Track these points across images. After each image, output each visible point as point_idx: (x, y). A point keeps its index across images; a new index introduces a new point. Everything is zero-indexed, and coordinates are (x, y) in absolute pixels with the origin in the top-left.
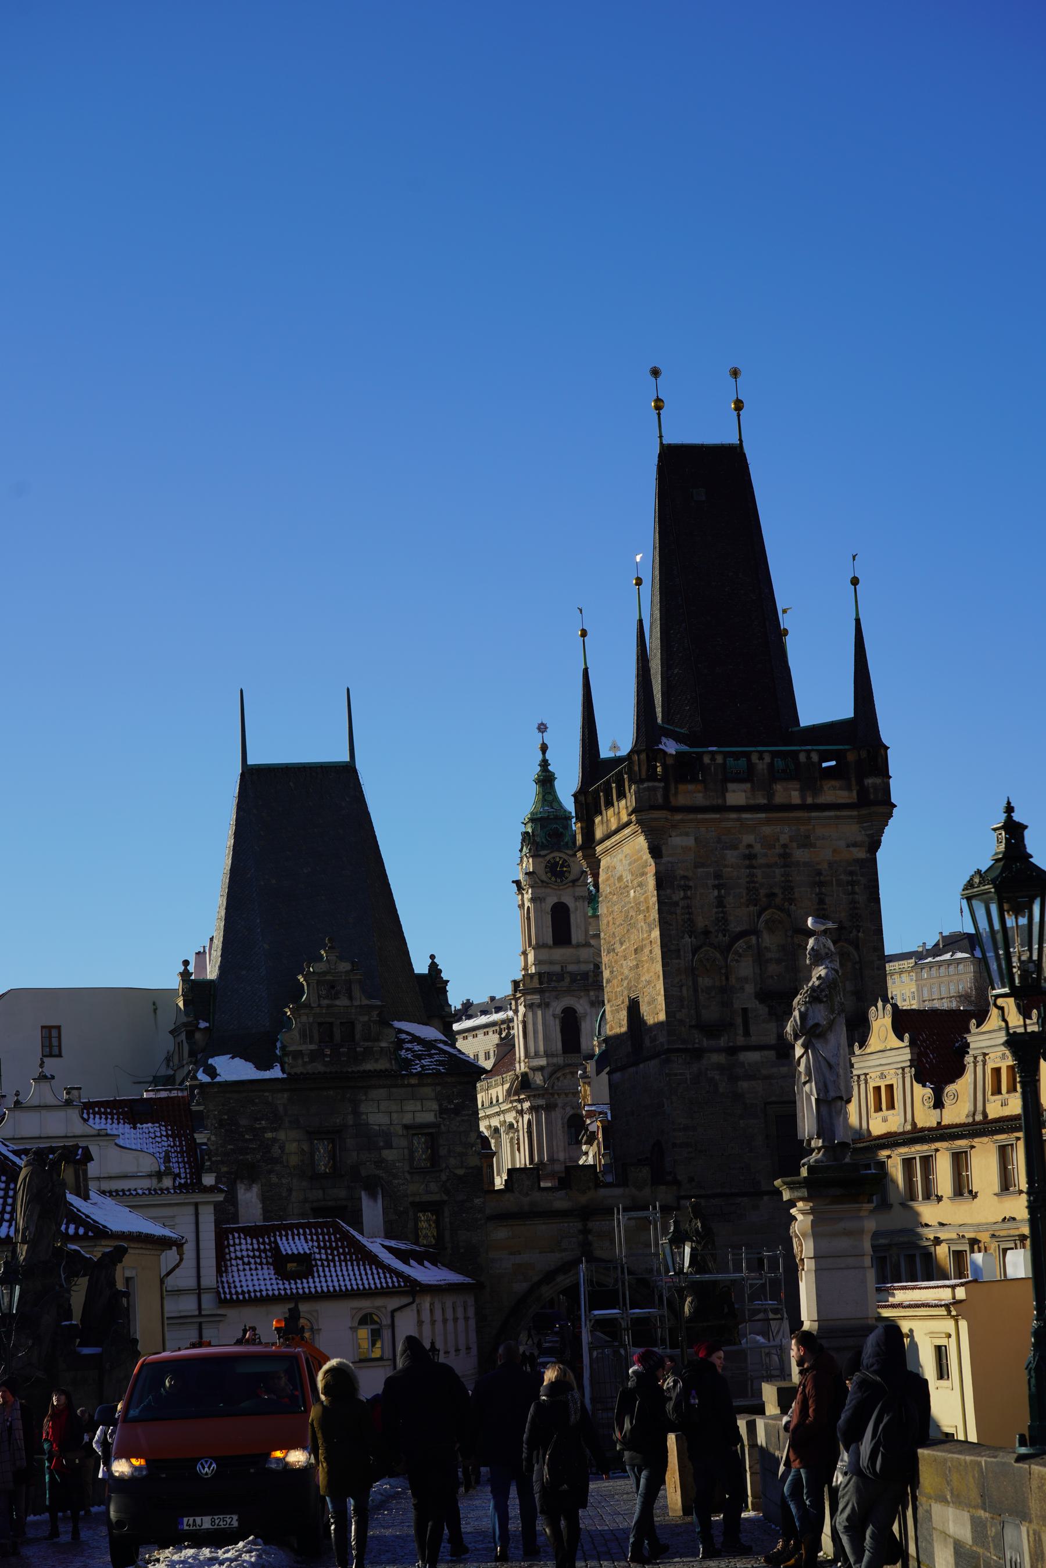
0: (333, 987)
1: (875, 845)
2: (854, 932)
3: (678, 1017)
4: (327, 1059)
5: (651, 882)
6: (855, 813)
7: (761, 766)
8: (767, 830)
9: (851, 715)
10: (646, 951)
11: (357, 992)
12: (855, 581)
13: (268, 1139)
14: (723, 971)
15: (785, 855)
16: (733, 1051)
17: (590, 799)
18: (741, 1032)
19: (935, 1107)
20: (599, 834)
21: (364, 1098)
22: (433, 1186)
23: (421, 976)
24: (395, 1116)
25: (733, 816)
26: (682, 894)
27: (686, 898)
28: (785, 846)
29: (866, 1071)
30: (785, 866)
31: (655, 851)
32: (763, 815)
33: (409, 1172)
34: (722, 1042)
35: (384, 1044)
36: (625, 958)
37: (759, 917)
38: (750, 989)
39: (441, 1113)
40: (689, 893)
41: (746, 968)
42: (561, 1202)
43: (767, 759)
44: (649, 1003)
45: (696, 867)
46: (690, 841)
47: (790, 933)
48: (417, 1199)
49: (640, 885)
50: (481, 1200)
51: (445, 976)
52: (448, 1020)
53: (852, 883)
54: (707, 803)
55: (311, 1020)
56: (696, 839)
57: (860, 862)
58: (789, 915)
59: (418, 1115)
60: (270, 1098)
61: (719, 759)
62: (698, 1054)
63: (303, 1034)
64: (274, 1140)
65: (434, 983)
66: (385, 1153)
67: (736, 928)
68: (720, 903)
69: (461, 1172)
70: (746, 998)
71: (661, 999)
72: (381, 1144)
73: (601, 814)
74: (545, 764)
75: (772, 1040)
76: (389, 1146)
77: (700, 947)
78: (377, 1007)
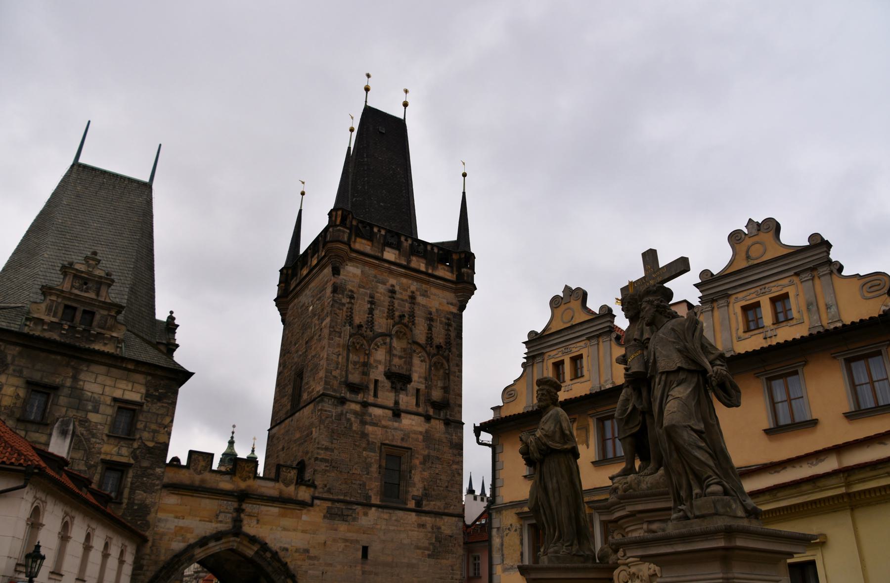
1: (462, 307)
2: (447, 352)
3: (334, 373)
5: (329, 290)
7: (406, 244)
8: (404, 280)
9: (455, 238)
11: (103, 292)
12: (464, 175)
15: (413, 298)
16: (365, 405)
17: (290, 272)
18: (372, 393)
21: (85, 369)
22: (125, 451)
24: (107, 389)
25: (386, 265)
28: (413, 292)
29: (544, 351)
33: (108, 436)
34: (360, 397)
35: (114, 334)
36: (297, 352)
37: (393, 326)
38: (381, 368)
39: (146, 397)
41: (380, 355)
42: (226, 484)
43: (410, 242)
44: (312, 370)
47: (410, 341)
48: (108, 458)
49: (319, 299)
50: (162, 470)
51: (176, 322)
54: (372, 253)
56: (362, 271)
57: (454, 315)
61: (383, 232)
62: (343, 401)
63: (49, 310)
68: (371, 312)
69: (151, 444)
70: (378, 373)
71: (323, 363)
72: (90, 408)
73: (296, 275)
74: (232, 437)
75: (391, 403)
76: (96, 410)
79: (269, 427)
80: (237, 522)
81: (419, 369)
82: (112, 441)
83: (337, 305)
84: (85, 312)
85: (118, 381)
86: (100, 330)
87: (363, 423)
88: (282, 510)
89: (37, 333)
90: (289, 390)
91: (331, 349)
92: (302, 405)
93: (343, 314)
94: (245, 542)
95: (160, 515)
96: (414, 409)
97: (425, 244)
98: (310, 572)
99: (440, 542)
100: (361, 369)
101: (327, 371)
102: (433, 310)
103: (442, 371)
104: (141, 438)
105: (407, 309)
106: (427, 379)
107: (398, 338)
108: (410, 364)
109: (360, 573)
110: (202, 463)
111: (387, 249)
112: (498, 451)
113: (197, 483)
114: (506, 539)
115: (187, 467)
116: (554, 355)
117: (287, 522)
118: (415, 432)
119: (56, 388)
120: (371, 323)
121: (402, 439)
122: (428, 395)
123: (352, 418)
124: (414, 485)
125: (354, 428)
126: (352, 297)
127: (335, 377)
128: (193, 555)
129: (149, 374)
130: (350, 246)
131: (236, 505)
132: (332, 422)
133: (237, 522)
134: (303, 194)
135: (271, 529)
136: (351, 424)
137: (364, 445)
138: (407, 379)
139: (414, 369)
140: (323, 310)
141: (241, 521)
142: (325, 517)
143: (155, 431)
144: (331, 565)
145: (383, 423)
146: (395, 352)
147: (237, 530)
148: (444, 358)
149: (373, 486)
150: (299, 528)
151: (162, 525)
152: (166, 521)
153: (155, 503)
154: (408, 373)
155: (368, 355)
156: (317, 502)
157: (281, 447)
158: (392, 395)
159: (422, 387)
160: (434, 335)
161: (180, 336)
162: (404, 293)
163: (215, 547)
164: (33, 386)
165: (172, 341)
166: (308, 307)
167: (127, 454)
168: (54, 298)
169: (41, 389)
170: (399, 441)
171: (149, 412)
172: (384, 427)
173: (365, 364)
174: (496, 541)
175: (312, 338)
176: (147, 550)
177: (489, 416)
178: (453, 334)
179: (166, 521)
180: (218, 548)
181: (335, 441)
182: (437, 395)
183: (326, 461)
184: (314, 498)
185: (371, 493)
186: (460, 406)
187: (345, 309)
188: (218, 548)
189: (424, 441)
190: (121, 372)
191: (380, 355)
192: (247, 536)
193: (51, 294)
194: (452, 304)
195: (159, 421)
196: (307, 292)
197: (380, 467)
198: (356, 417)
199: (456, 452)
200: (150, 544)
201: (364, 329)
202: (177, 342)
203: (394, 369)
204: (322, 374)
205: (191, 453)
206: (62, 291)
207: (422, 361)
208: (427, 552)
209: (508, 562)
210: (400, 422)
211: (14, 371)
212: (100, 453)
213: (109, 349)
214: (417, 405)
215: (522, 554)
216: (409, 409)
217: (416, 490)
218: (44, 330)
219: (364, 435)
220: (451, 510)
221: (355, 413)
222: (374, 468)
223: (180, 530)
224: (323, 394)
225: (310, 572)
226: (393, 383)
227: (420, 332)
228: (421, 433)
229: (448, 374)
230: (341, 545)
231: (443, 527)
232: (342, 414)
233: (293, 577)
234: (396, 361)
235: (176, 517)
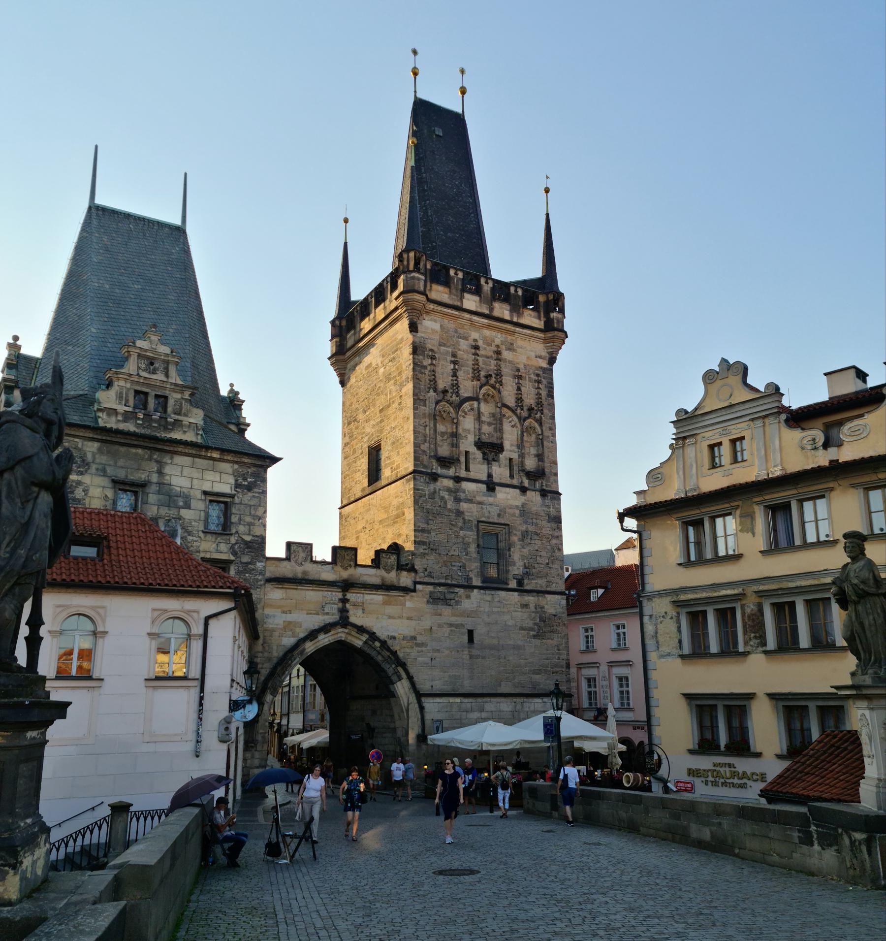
0: (152, 364)
1: (552, 361)
2: (539, 414)
3: (422, 447)
4: (140, 422)
6: (542, 335)
7: (487, 288)
8: (487, 332)
10: (396, 405)
13: (73, 481)
14: (455, 421)
15: (498, 353)
17: (344, 323)
18: (463, 467)
19: (826, 446)
20: (350, 343)
21: (169, 461)
22: (223, 547)
23: (224, 398)
24: (195, 482)
25: (467, 316)
26: (430, 361)
27: (432, 364)
28: (497, 346)
30: (498, 359)
31: (413, 327)
32: (485, 321)
33: (203, 532)
34: (451, 472)
37: (481, 388)
38: (471, 439)
39: (236, 487)
40: (434, 362)
42: (328, 575)
43: (491, 284)
44: (393, 443)
45: (440, 345)
46: (437, 326)
47: (499, 405)
48: (208, 556)
50: (263, 564)
51: (241, 397)
52: (242, 427)
53: (539, 382)
55: (128, 385)
56: (441, 326)
57: (544, 370)
58: (499, 392)
59: (215, 484)
60: (80, 445)
61: (460, 275)
62: (434, 477)
63: (120, 397)
64: (79, 483)
65: (234, 403)
66: (184, 513)
67: (465, 393)
68: (455, 375)
69: (248, 538)
70: (468, 444)
71: (410, 436)
72: (181, 504)
73: (354, 328)
75: (485, 478)
76: (188, 506)
77: (441, 401)
78: (189, 388)
79: (340, 505)
80: (343, 612)
81: (510, 436)
82: (209, 537)
83: (418, 369)
84: (157, 396)
85: (205, 472)
86: (177, 417)
87: (458, 500)
88: (385, 597)
89: (114, 427)
90: (363, 463)
91: (417, 420)
92: (383, 482)
93: (426, 378)
94: (353, 633)
95: (267, 611)
96: (508, 481)
97: (507, 285)
98: (419, 659)
99: (544, 621)
100: (449, 440)
101: (416, 446)
102: (521, 367)
103: (534, 436)
104: (237, 532)
105: (493, 367)
106: (521, 446)
107: (486, 401)
108: (501, 431)
109: (468, 657)
110: (302, 555)
111: (466, 295)
112: (645, 536)
113: (300, 576)
114: (660, 627)
115: (288, 559)
116: (710, 436)
117: (391, 610)
118: (511, 507)
119: (143, 485)
120: (456, 386)
121: (499, 515)
122: (522, 464)
123: (446, 495)
124: (514, 564)
125: (449, 507)
126: (433, 358)
127: (424, 451)
128: (304, 649)
129: (236, 462)
130: (427, 296)
131: (340, 595)
132: (426, 502)
133: (343, 612)
134: (346, 221)
135: (377, 618)
136: (445, 503)
137: (460, 524)
138: (499, 448)
139: (505, 436)
140: (400, 374)
141: (348, 611)
142: (428, 602)
143: (250, 524)
144: (438, 651)
145: (478, 499)
146: (483, 418)
147: (344, 621)
148: (536, 421)
149: (473, 567)
150: (404, 615)
151: (270, 620)
152: (274, 616)
153: (261, 599)
154: (499, 442)
155: (457, 424)
156: (419, 587)
157: (360, 527)
158: (485, 467)
159: (515, 456)
160: (524, 396)
161: (247, 413)
162: (488, 348)
163: (324, 640)
164: (120, 485)
165: (242, 420)
166: (376, 369)
167: (226, 550)
168: (122, 383)
169: (128, 488)
170: (496, 517)
171: (241, 503)
172: (480, 503)
173: (455, 435)
174: (649, 628)
175: (389, 406)
176: (259, 648)
177: (632, 501)
178: (544, 393)
179: (274, 616)
180: (326, 640)
181: (431, 522)
182: (531, 464)
183: (424, 543)
184: (415, 583)
185: (471, 575)
186: (556, 474)
187: (427, 372)
188: (326, 640)
189: (521, 515)
190: (206, 462)
191: (468, 423)
192: (354, 626)
193: (118, 379)
194: (540, 357)
195: (253, 512)
196: (373, 351)
197: (478, 546)
198: (449, 495)
199: (554, 525)
200: (261, 641)
201: (449, 394)
202: (247, 421)
203: (485, 438)
204: (410, 449)
205: (289, 545)
206: (130, 375)
207: (512, 426)
208: (532, 633)
209: (664, 649)
210: (495, 496)
211: (97, 469)
212: (199, 552)
213: (190, 437)
214: (512, 476)
215: (680, 642)
216: (503, 481)
217: (517, 569)
218: (119, 421)
219: (459, 513)
220: (553, 588)
221: (449, 490)
222: (473, 548)
223: (289, 626)
224: (414, 472)
225: (419, 659)
226: (484, 454)
227: (509, 395)
228: (517, 507)
229: (542, 439)
230: (447, 630)
231: (546, 607)
232: (435, 492)
233: (403, 665)
234: (486, 429)
235: (283, 612)
